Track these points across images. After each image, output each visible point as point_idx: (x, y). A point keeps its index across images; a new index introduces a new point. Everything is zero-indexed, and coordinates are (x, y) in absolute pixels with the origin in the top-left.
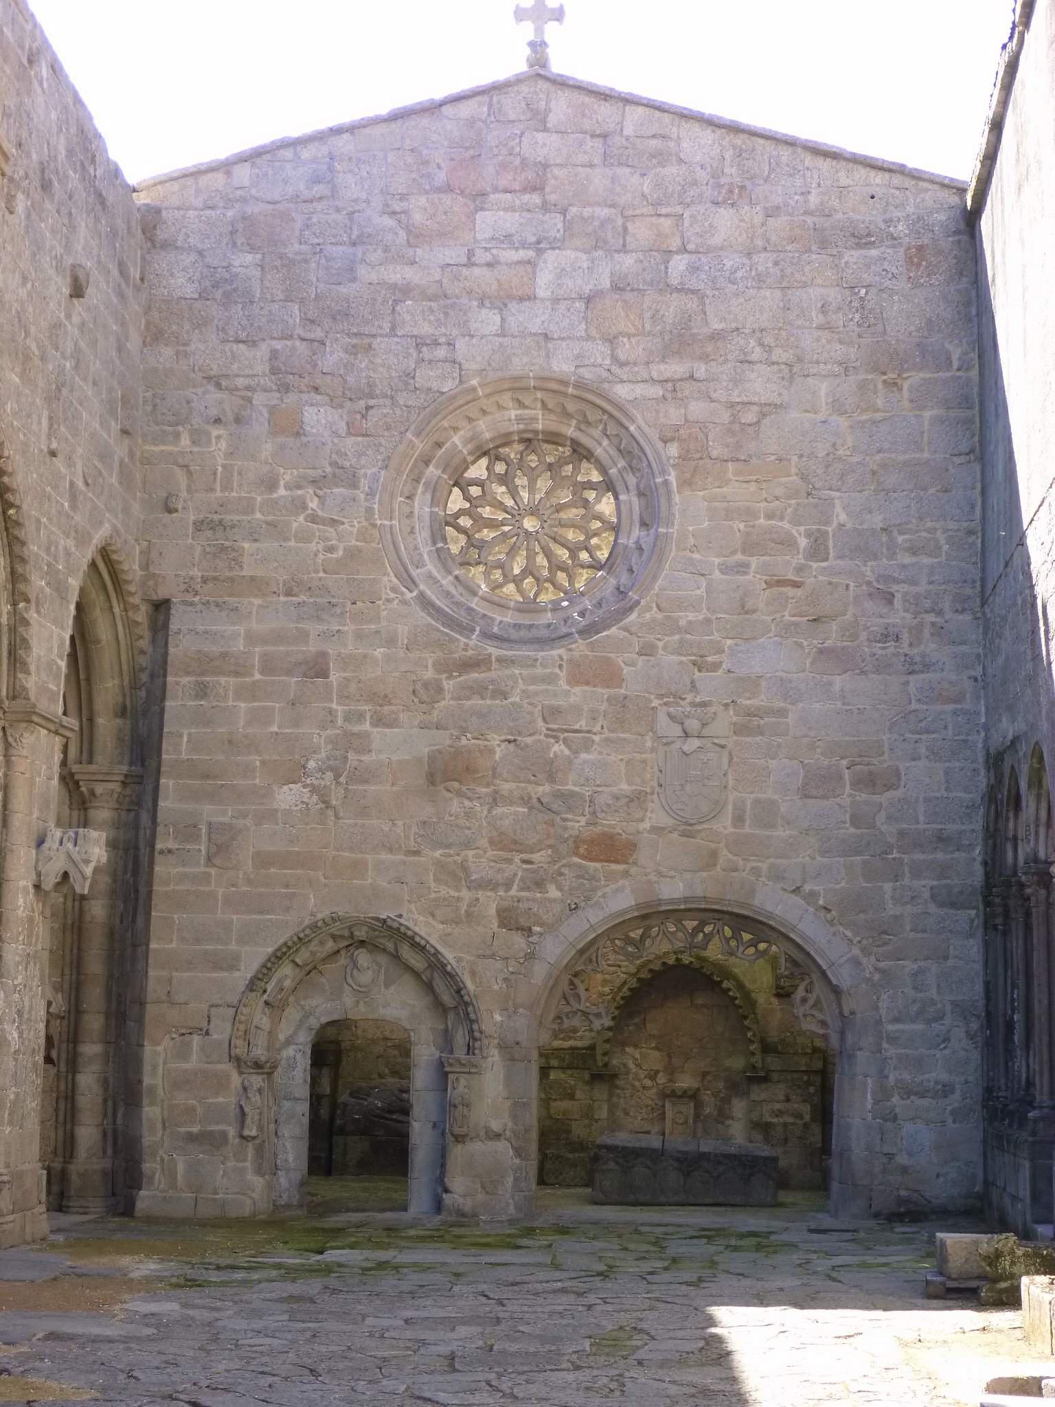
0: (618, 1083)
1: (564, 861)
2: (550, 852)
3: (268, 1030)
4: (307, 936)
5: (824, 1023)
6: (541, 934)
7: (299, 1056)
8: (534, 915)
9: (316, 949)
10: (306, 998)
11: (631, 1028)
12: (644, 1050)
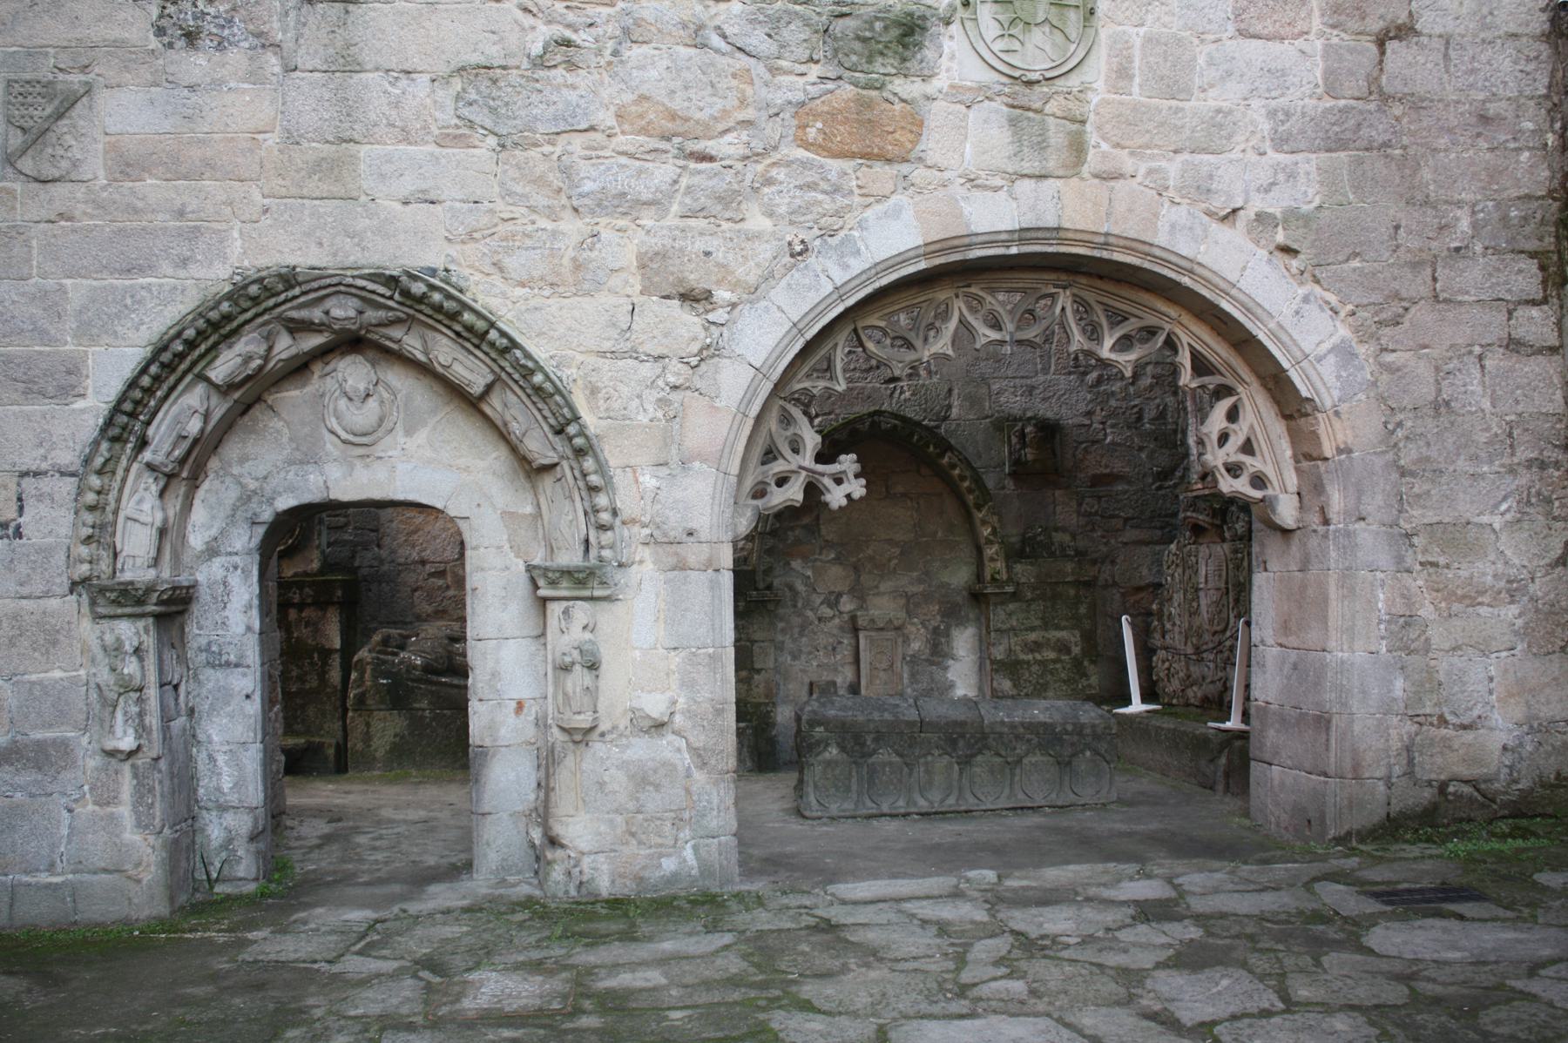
0: (781, 611)
1: (776, 156)
2: (745, 138)
3: (158, 523)
4: (228, 318)
5: (1259, 481)
6: (734, 305)
7: (235, 580)
8: (718, 265)
9: (251, 348)
10: (243, 460)
11: (797, 532)
12: (819, 564)
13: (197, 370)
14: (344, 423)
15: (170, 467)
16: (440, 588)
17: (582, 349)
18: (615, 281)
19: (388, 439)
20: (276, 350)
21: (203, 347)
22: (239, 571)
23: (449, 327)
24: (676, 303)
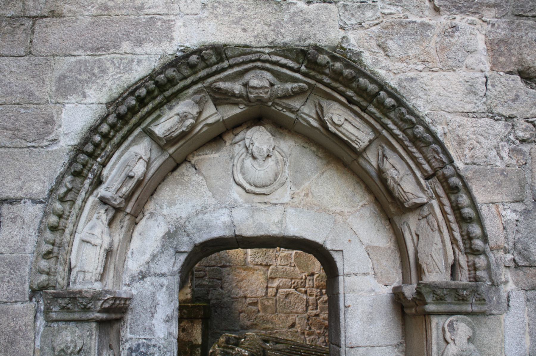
3: (106, 246)
4: (171, 82)
9: (185, 109)
13: (143, 125)
14: (248, 178)
15: (118, 201)
16: (254, 312)
17: (450, 110)
18: (470, 60)
19: (280, 191)
20: (204, 116)
21: (150, 106)
22: (165, 288)
23: (342, 94)
24: (518, 78)
